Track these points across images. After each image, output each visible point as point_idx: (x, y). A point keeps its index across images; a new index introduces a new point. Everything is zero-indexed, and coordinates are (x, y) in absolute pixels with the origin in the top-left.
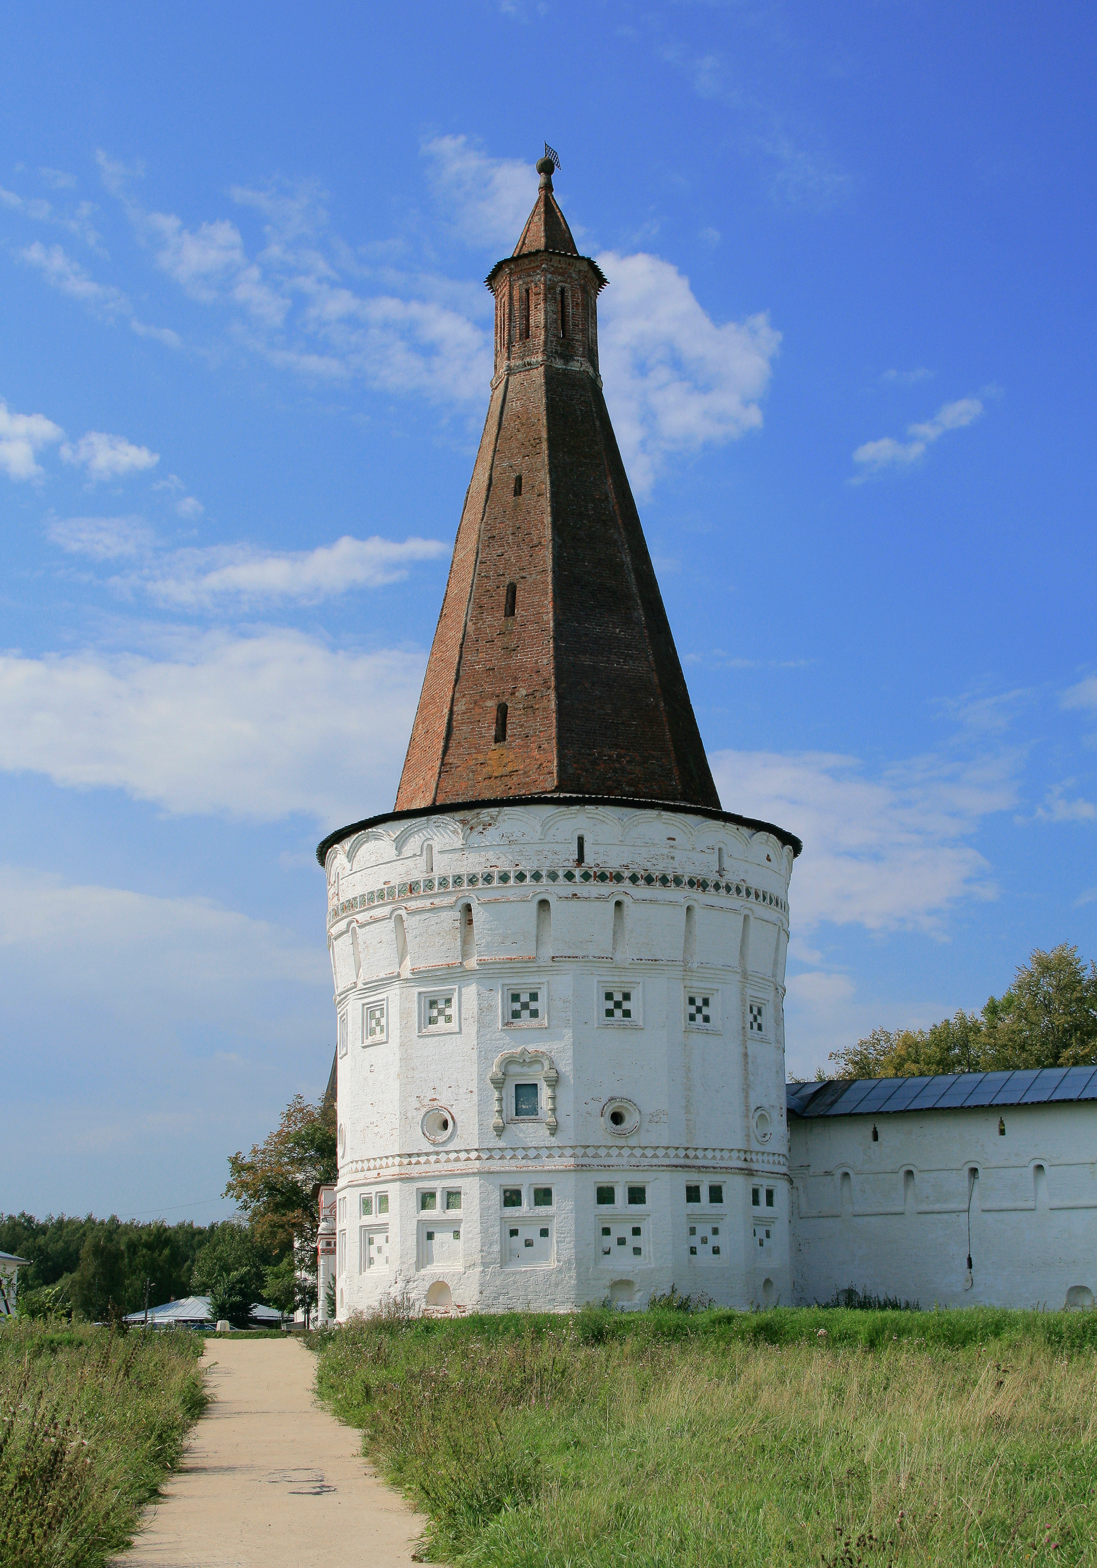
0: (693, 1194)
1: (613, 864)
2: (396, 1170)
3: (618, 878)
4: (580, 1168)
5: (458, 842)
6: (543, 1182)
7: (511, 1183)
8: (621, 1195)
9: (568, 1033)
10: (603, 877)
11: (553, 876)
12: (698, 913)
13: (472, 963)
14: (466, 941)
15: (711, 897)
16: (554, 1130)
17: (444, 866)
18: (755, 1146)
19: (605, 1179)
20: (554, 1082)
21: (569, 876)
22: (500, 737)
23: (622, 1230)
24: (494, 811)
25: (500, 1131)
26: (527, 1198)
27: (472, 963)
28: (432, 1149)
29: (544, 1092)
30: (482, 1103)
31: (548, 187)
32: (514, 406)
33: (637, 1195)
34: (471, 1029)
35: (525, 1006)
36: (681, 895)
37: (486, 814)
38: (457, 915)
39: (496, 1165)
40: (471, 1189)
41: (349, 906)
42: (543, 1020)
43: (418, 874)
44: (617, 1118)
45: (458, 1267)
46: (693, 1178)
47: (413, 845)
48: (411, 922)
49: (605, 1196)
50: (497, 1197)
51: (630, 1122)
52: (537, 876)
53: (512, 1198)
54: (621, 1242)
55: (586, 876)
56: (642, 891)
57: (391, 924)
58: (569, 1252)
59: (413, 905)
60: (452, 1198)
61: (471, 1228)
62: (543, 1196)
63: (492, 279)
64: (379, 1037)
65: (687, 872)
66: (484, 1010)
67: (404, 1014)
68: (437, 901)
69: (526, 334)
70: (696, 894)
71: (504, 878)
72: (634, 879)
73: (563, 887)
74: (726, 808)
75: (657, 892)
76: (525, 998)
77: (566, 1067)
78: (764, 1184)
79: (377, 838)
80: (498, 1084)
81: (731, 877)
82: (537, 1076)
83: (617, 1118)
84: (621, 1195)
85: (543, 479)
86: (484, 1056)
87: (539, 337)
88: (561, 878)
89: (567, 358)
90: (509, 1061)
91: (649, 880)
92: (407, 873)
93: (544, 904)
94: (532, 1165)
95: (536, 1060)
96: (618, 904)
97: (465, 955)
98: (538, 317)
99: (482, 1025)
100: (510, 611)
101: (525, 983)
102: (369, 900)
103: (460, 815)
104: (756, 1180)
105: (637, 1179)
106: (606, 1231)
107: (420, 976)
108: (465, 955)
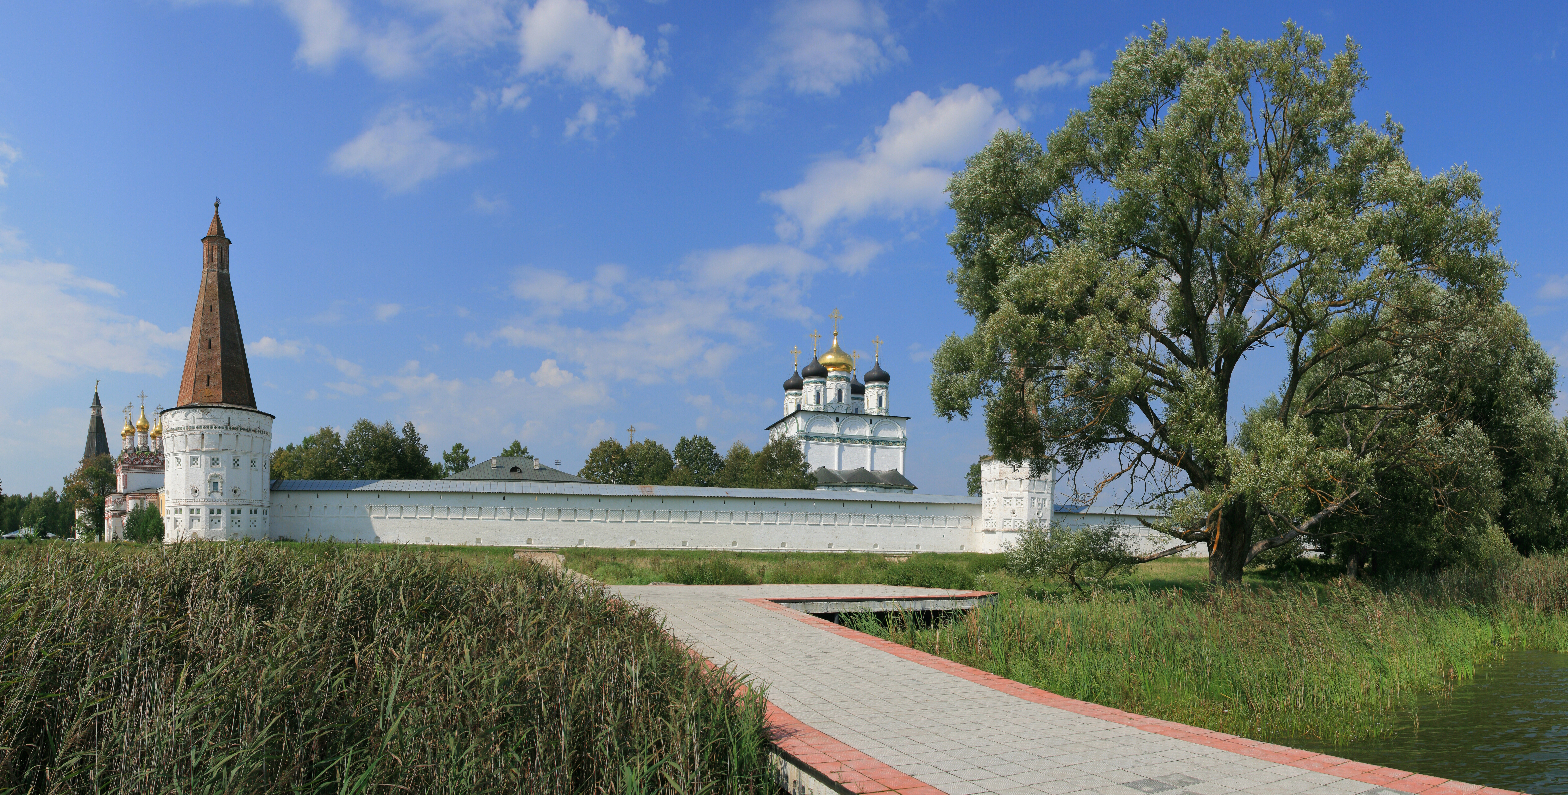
0: (251, 512)
4: (228, 504)
5: (201, 416)
6: (219, 508)
7: (212, 508)
8: (236, 512)
9: (225, 469)
13: (204, 449)
14: (202, 443)
16: (222, 495)
19: (232, 507)
20: (222, 482)
23: (236, 521)
25: (210, 494)
26: (215, 512)
27: (204, 449)
29: (220, 485)
30: (206, 487)
32: (210, 282)
33: (239, 512)
34: (203, 467)
39: (208, 503)
40: (203, 509)
41: (172, 430)
42: (220, 465)
43: (191, 424)
44: (235, 492)
45: (199, 529)
47: (190, 416)
48: (189, 437)
49: (232, 512)
50: (209, 511)
51: (238, 493)
53: (212, 512)
57: (183, 437)
58: (225, 526)
60: (198, 511)
61: (203, 519)
62: (219, 511)
63: (202, 240)
66: (206, 462)
67: (187, 461)
69: (212, 260)
77: (225, 478)
78: (265, 509)
80: (209, 482)
82: (218, 480)
83: (235, 492)
84: (236, 512)
85: (217, 308)
86: (206, 475)
87: (216, 262)
89: (222, 269)
90: (212, 476)
94: (217, 503)
95: (218, 476)
97: (202, 447)
98: (216, 256)
99: (206, 466)
102: (178, 429)
107: (191, 452)
108: (202, 447)
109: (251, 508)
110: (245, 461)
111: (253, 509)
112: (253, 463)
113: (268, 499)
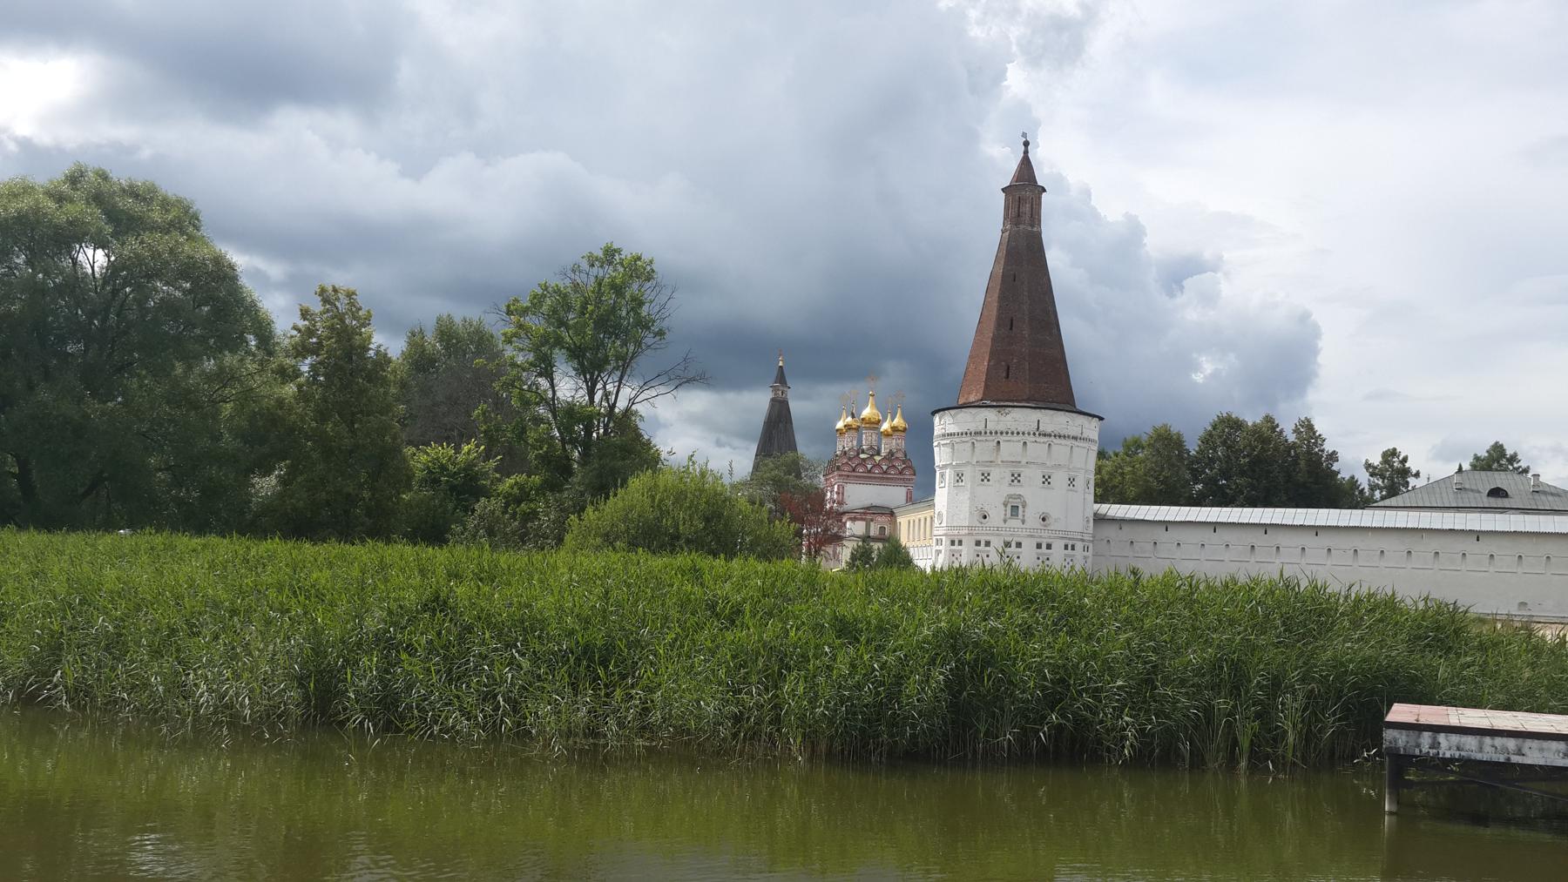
0: (1066, 547)
1: (1049, 430)
2: (967, 532)
3: (1050, 435)
8: (1044, 546)
10: (1045, 435)
11: (1029, 434)
12: (1075, 449)
15: (1081, 444)
16: (1023, 522)
17: (990, 426)
18: (1086, 531)
21: (1034, 434)
22: (1007, 377)
24: (1010, 409)
28: (979, 525)
29: (1021, 509)
31: (1026, 152)
33: (1049, 547)
35: (1016, 478)
36: (1069, 442)
37: (1007, 410)
38: (995, 445)
43: (981, 428)
44: (1044, 519)
46: (1067, 541)
52: (1023, 433)
54: (1043, 562)
55: (1040, 435)
56: (1057, 441)
57: (970, 444)
59: (979, 438)
64: (960, 484)
65: (1072, 434)
68: (988, 438)
70: (1073, 442)
71: (1012, 433)
72: (1055, 436)
73: (1032, 438)
74: (1079, 407)
75: (1063, 441)
76: (1016, 476)
79: (966, 412)
80: (1005, 505)
81: (1085, 435)
84: (1044, 546)
88: (1032, 436)
89: (1033, 226)
91: (1060, 436)
92: (977, 427)
93: (1025, 443)
96: (1050, 444)
100: (1011, 329)
101: (1017, 470)
103: (998, 409)
104: (1085, 543)
105: (1050, 541)
106: (1038, 558)
109: (1067, 541)
110: (1059, 478)
111: (1070, 543)
112: (1072, 481)
113: (1091, 530)
